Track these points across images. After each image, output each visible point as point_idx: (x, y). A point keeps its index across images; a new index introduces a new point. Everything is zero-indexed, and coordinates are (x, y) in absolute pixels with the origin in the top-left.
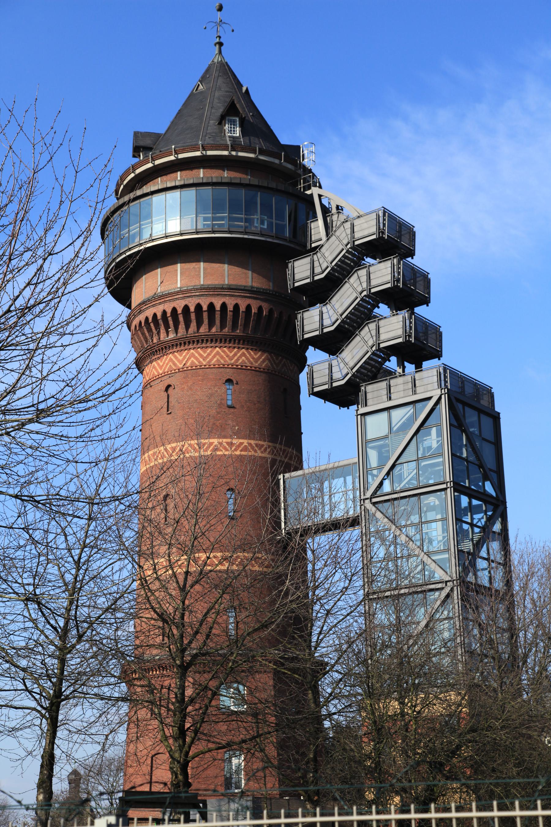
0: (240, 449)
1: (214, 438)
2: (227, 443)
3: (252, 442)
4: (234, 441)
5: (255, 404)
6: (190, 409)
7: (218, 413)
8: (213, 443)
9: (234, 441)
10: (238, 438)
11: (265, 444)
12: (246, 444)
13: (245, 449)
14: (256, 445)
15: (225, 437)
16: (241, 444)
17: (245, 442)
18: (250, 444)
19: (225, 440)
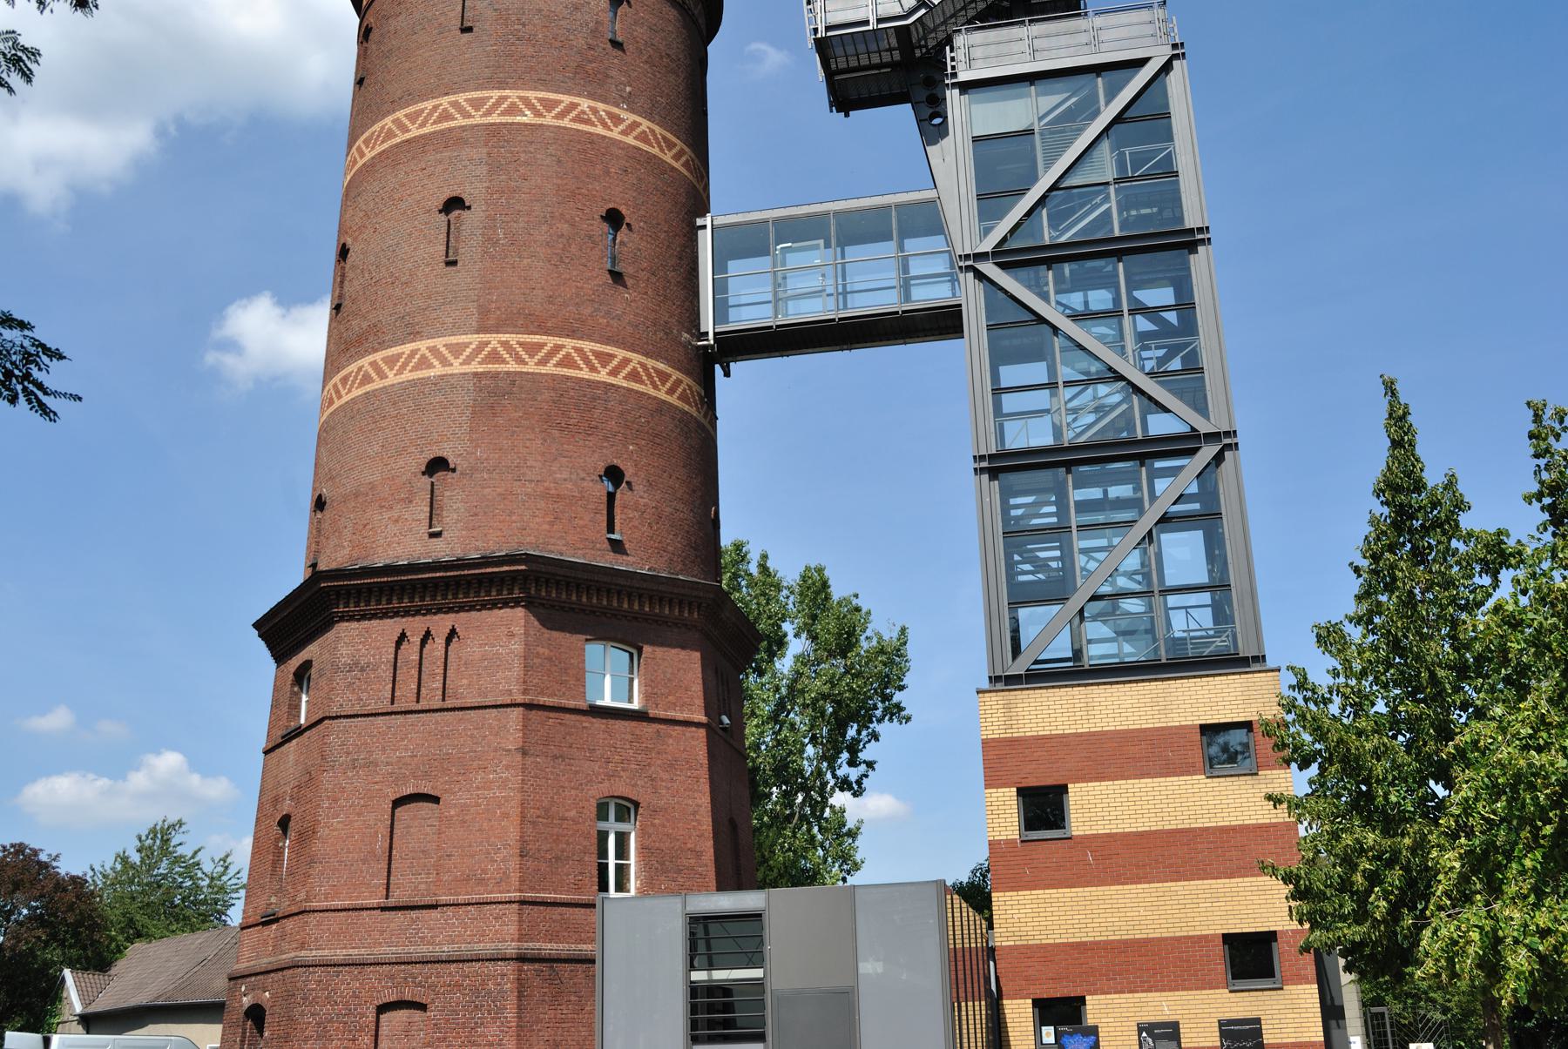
0: (635, 133)
1: (579, 95)
2: (608, 113)
3: (657, 129)
4: (624, 115)
5: (661, 57)
6: (524, 25)
7: (590, 48)
8: (577, 105)
9: (624, 115)
10: (631, 110)
11: (680, 144)
12: (643, 128)
13: (642, 137)
14: (664, 138)
15: (605, 101)
16: (635, 125)
17: (645, 124)
18: (653, 131)
19: (600, 106)
